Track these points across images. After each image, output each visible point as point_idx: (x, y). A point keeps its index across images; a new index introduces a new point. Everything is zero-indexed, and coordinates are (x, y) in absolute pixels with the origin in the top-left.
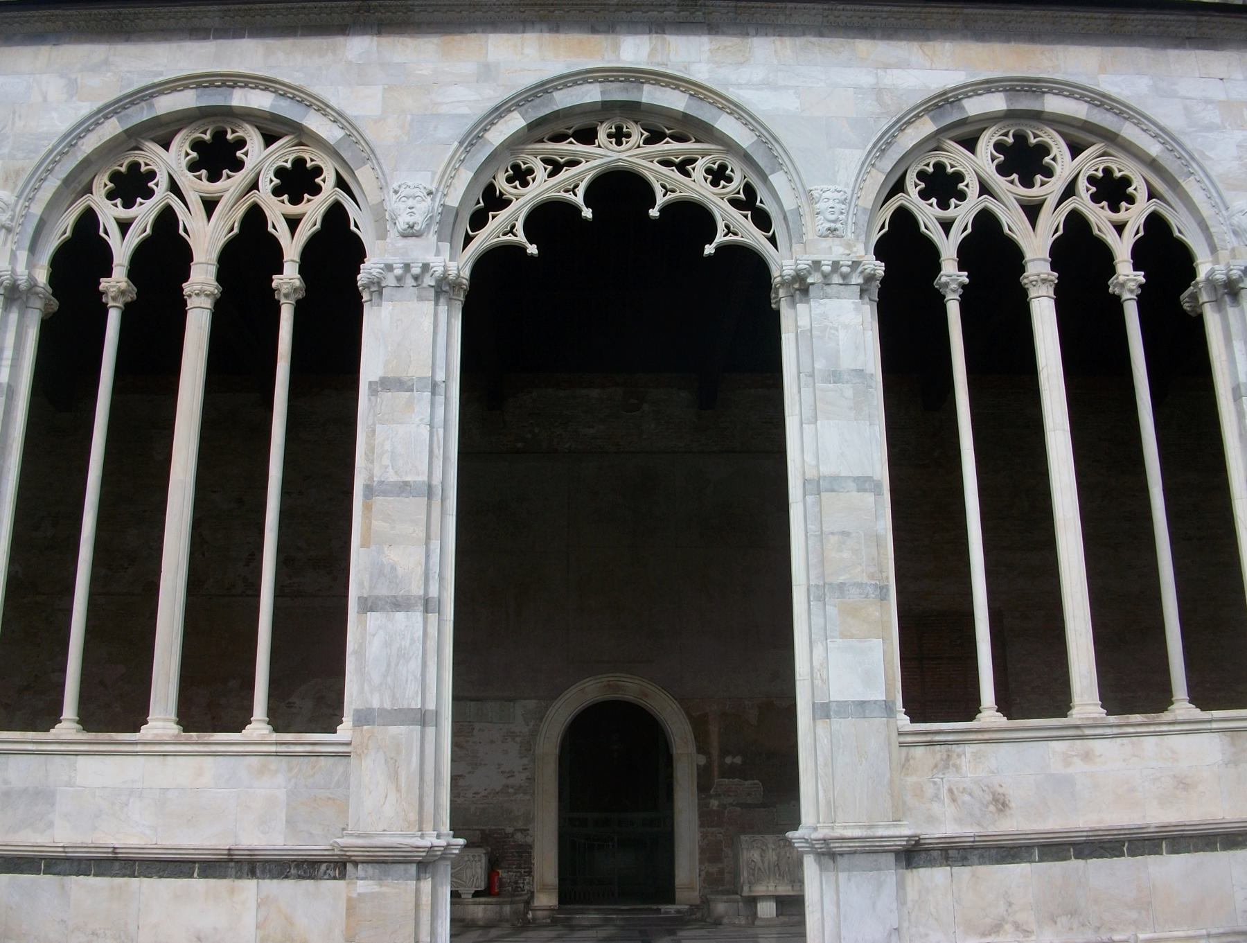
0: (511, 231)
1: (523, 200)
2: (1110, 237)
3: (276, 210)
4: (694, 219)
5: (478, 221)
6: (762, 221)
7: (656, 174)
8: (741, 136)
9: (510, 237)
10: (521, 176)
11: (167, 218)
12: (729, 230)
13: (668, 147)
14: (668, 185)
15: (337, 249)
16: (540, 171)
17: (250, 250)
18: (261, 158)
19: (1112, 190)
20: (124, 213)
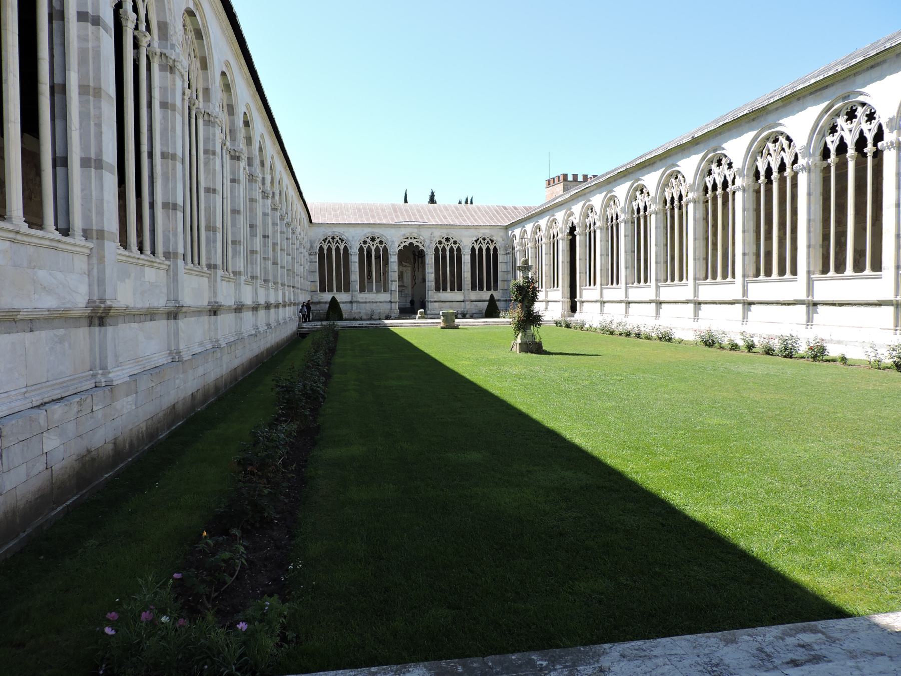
4: (418, 246)
14: (415, 244)
15: (385, 250)
17: (377, 249)
18: (378, 240)
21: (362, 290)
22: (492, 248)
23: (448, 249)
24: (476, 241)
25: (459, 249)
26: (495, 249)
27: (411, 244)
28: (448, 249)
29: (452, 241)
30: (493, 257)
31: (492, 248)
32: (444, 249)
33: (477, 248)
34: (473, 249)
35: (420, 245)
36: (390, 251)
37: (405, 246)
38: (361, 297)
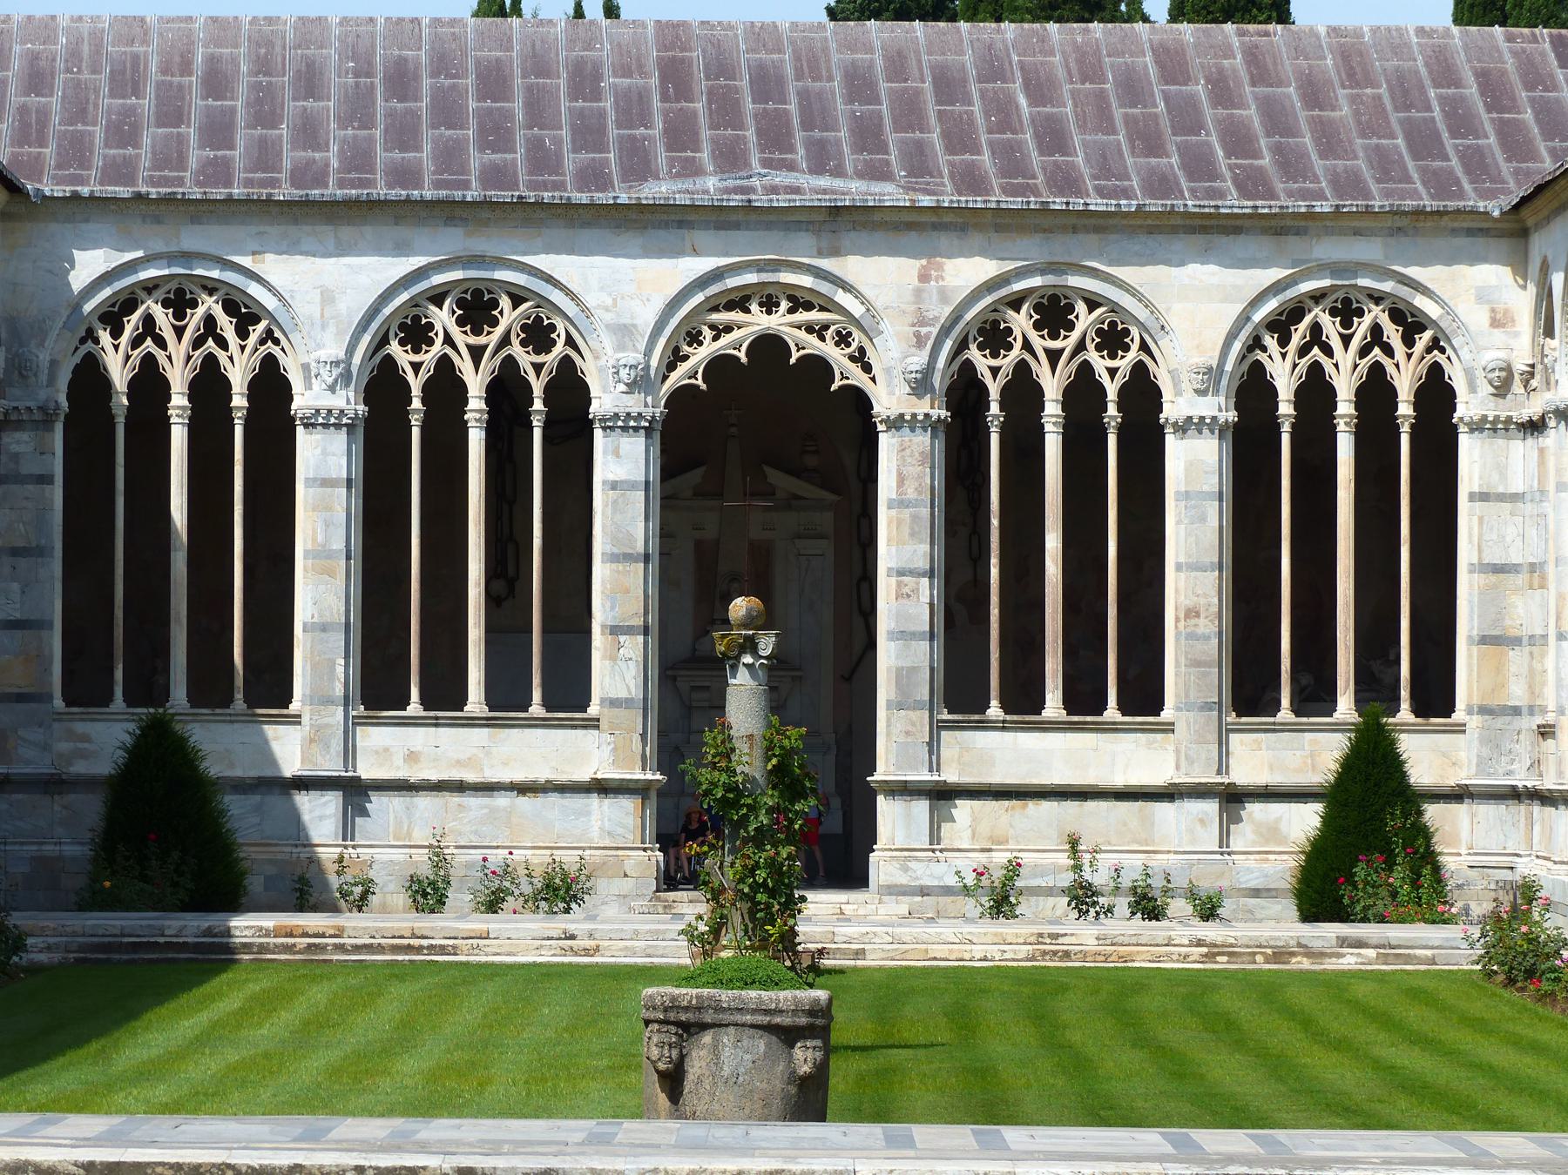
0: (694, 376)
1: (700, 355)
2: (1105, 380)
3: (525, 359)
4: (819, 367)
5: (671, 367)
6: (867, 368)
7: (793, 336)
8: (857, 309)
9: (693, 381)
10: (695, 339)
11: (444, 363)
12: (843, 377)
13: (802, 316)
15: (569, 389)
16: (708, 333)
19: (1113, 340)
20: (416, 358)
21: (379, 690)
22: (1405, 381)
23: (1052, 385)
24: (1280, 326)
25: (1142, 393)
26: (1436, 393)
27: (769, 346)
28: (1052, 385)
29: (1084, 320)
30: (1417, 450)
31: (1405, 381)
32: (1023, 390)
33: (1284, 377)
34: (1253, 390)
35: (836, 356)
36: (604, 399)
37: (719, 366)
38: (386, 749)
